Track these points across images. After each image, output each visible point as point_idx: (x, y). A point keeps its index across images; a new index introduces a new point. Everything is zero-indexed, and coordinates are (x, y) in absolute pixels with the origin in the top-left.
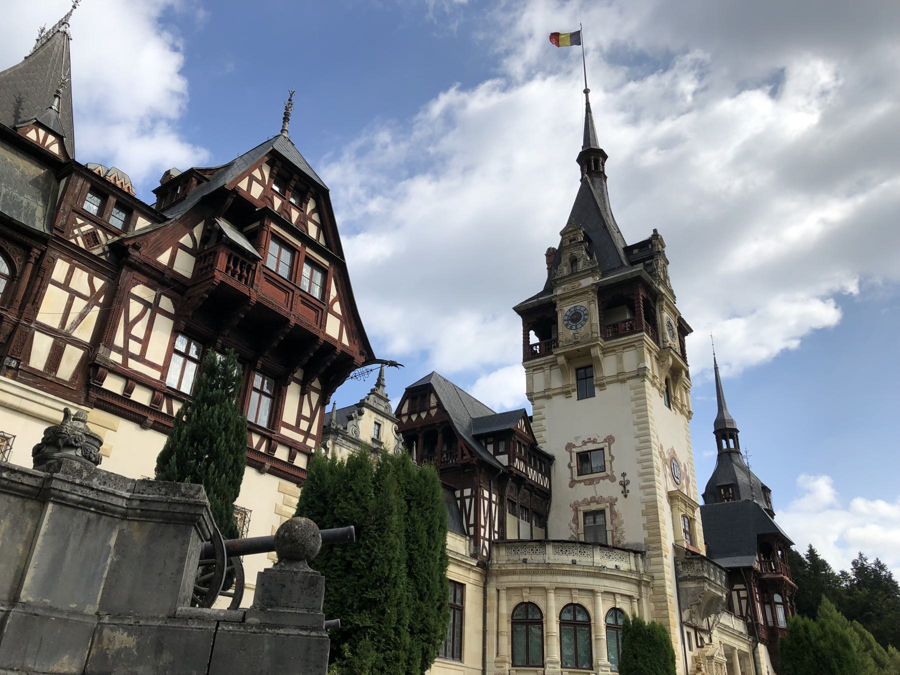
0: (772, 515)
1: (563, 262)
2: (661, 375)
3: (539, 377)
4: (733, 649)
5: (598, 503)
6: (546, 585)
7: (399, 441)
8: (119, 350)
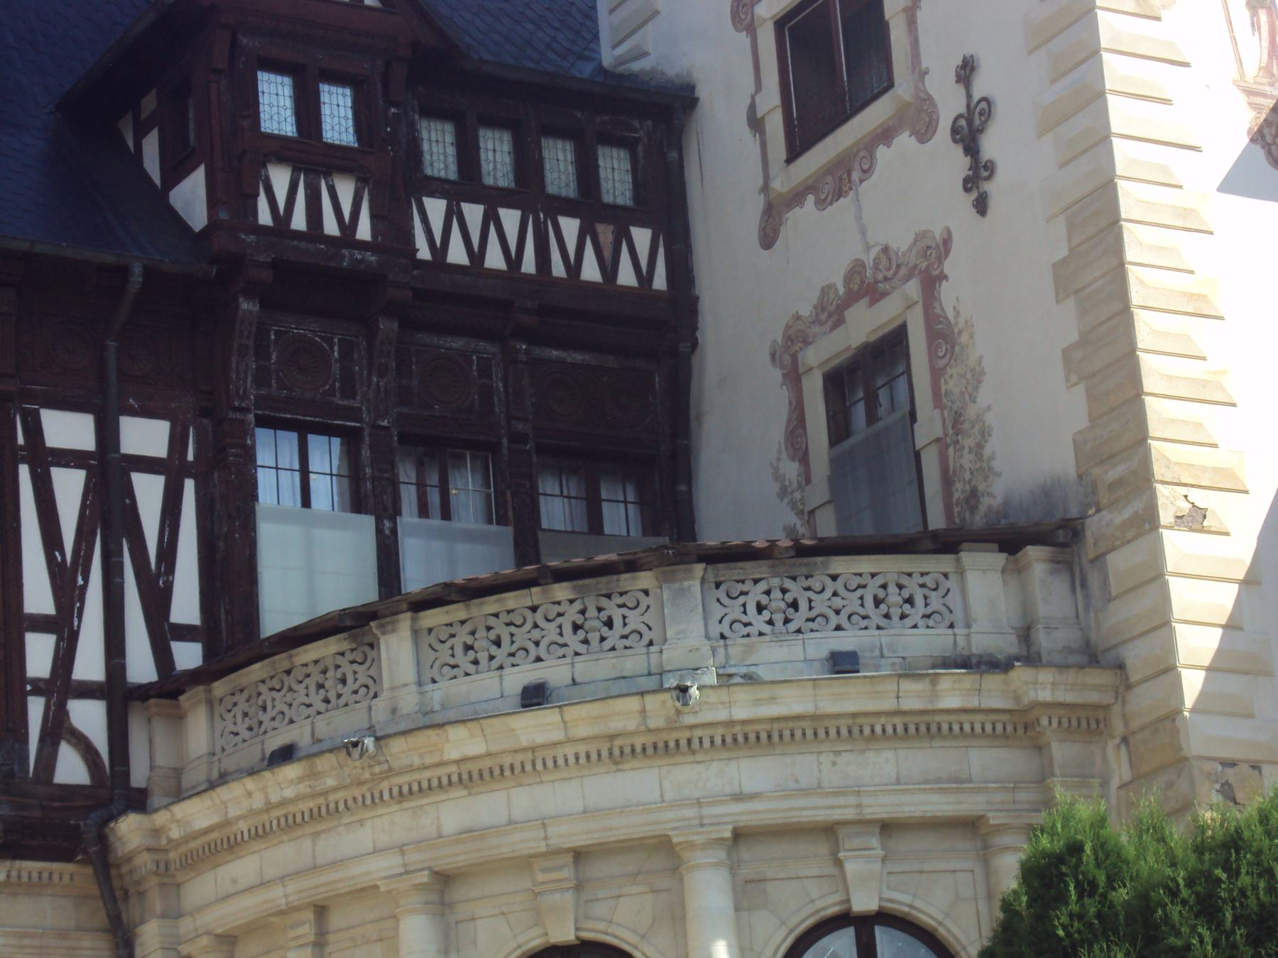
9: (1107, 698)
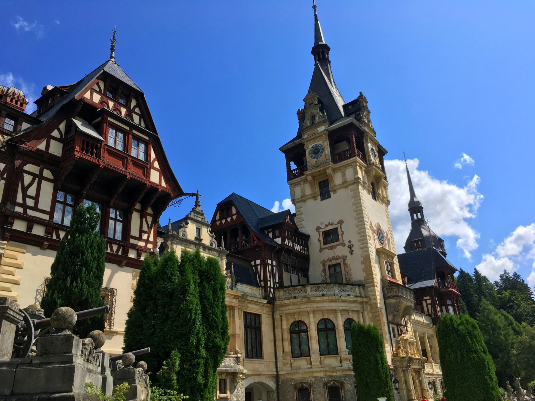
0: (445, 254)
1: (306, 118)
2: (369, 181)
3: (298, 190)
4: (424, 334)
5: (336, 259)
7: (212, 237)
8: (20, 205)
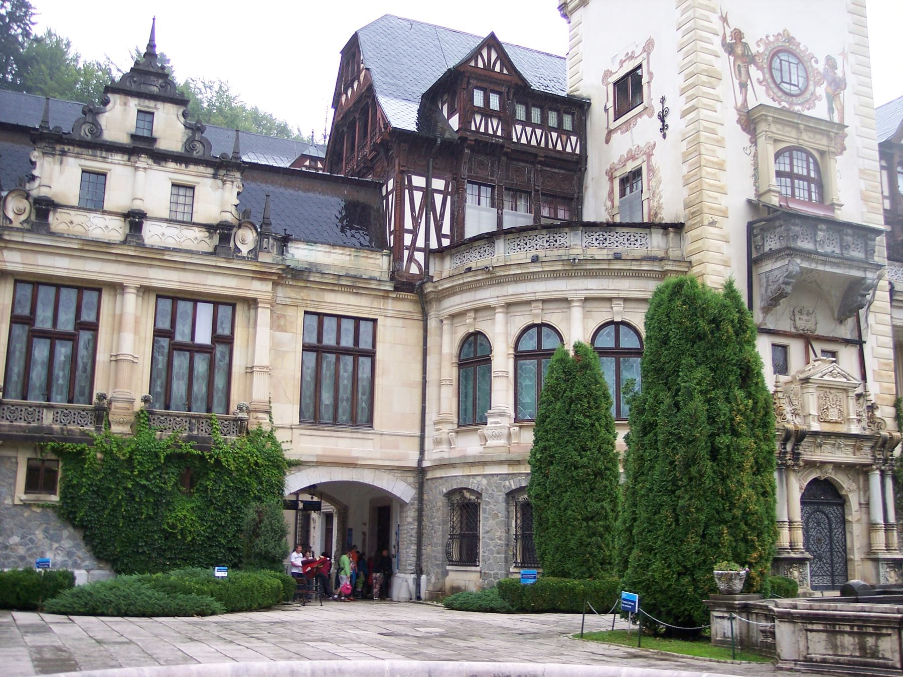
5: (633, 158)
6: (492, 302)
9: (686, 270)
